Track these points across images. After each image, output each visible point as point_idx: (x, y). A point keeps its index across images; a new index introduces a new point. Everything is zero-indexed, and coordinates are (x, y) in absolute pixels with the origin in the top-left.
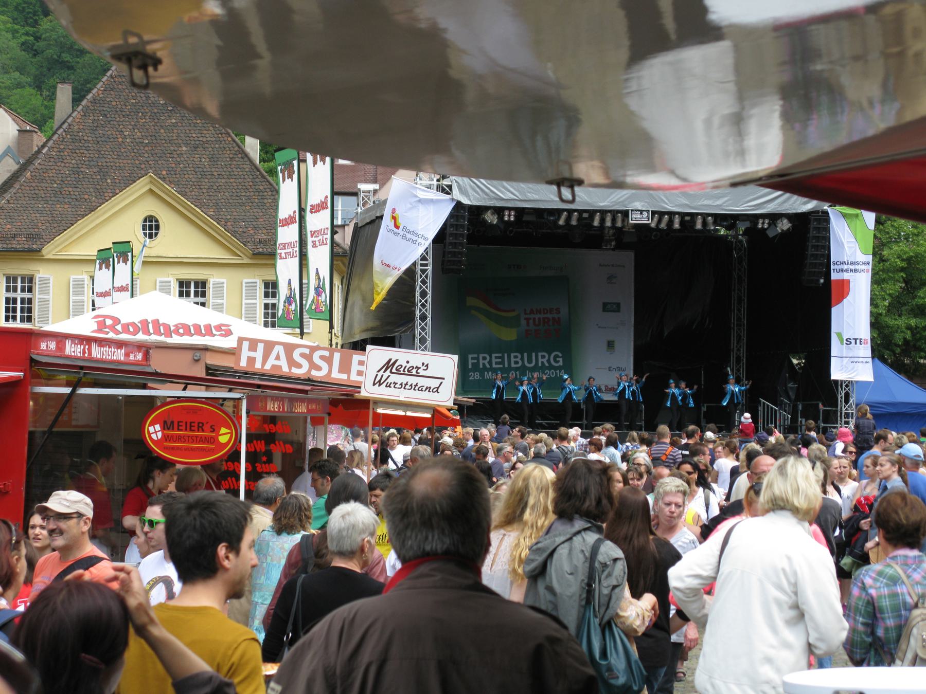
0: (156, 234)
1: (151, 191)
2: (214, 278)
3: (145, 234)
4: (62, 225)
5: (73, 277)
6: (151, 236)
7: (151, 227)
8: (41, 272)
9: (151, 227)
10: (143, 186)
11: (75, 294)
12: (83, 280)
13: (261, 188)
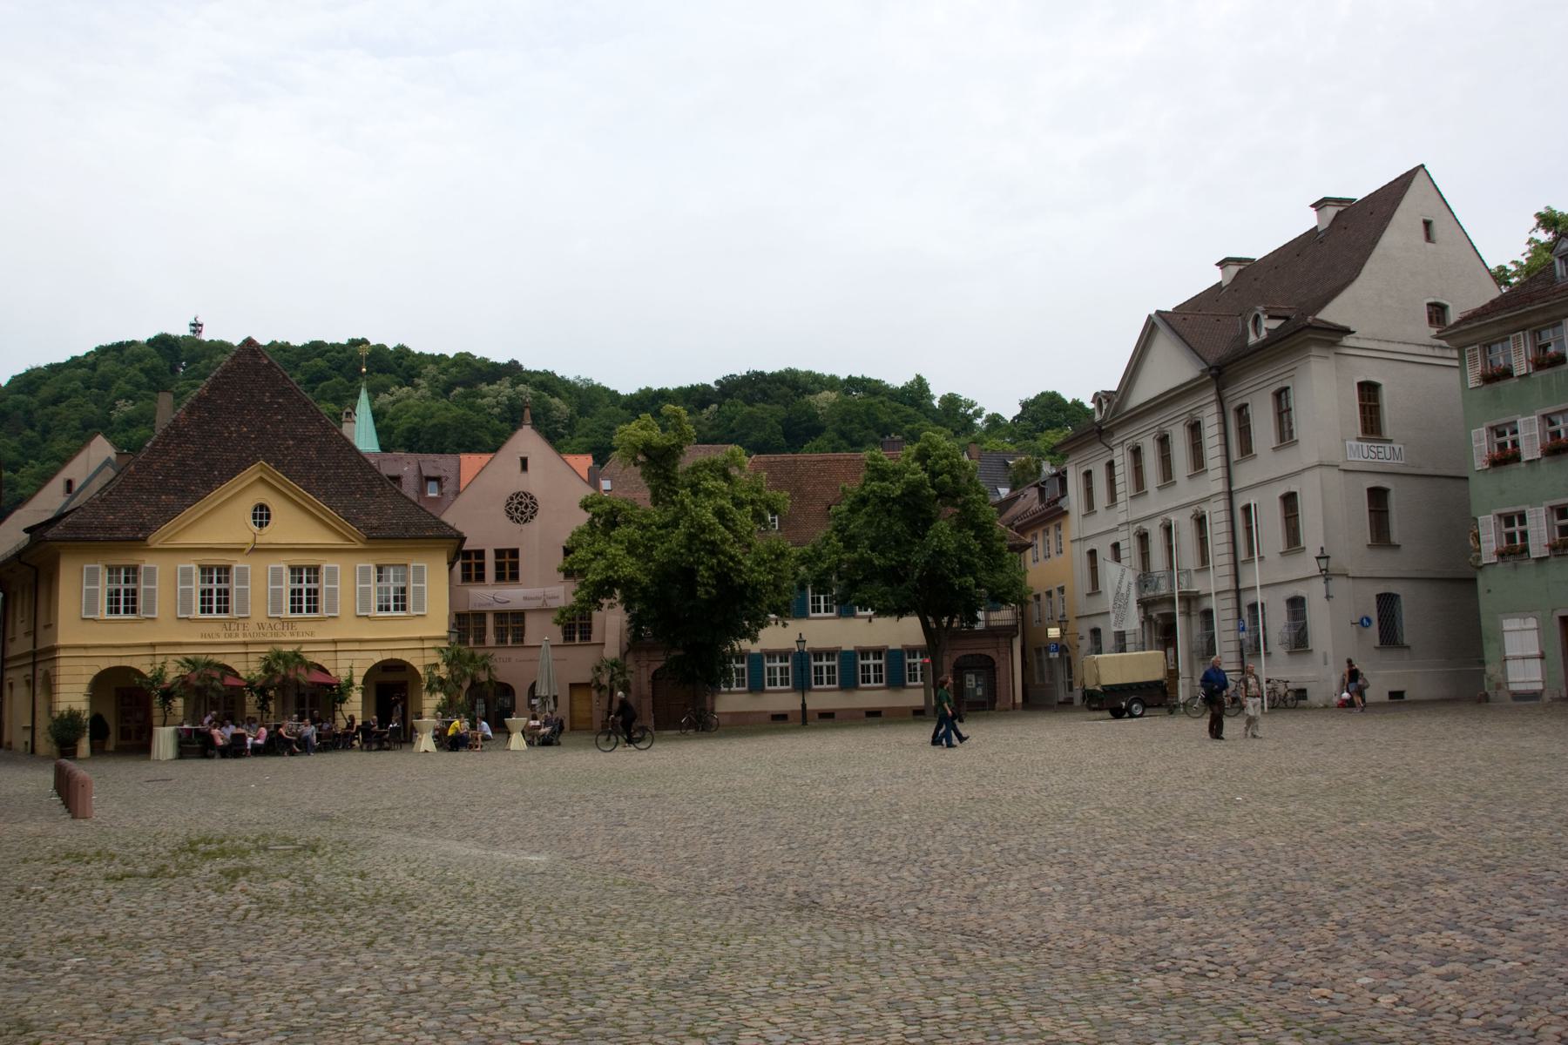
0: (267, 524)
1: (261, 478)
2: (327, 563)
3: (255, 523)
4: (168, 514)
5: (180, 566)
6: (261, 525)
7: (262, 515)
8: (147, 562)
9: (262, 515)
10: (254, 474)
11: (183, 583)
12: (191, 568)
13: (370, 477)
